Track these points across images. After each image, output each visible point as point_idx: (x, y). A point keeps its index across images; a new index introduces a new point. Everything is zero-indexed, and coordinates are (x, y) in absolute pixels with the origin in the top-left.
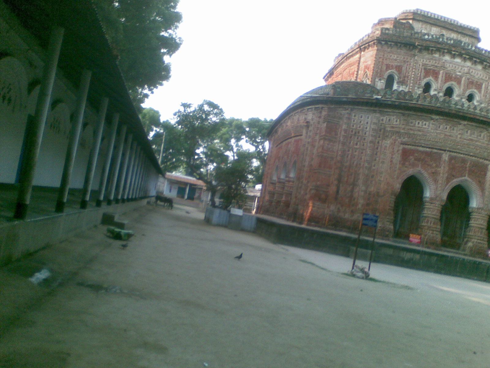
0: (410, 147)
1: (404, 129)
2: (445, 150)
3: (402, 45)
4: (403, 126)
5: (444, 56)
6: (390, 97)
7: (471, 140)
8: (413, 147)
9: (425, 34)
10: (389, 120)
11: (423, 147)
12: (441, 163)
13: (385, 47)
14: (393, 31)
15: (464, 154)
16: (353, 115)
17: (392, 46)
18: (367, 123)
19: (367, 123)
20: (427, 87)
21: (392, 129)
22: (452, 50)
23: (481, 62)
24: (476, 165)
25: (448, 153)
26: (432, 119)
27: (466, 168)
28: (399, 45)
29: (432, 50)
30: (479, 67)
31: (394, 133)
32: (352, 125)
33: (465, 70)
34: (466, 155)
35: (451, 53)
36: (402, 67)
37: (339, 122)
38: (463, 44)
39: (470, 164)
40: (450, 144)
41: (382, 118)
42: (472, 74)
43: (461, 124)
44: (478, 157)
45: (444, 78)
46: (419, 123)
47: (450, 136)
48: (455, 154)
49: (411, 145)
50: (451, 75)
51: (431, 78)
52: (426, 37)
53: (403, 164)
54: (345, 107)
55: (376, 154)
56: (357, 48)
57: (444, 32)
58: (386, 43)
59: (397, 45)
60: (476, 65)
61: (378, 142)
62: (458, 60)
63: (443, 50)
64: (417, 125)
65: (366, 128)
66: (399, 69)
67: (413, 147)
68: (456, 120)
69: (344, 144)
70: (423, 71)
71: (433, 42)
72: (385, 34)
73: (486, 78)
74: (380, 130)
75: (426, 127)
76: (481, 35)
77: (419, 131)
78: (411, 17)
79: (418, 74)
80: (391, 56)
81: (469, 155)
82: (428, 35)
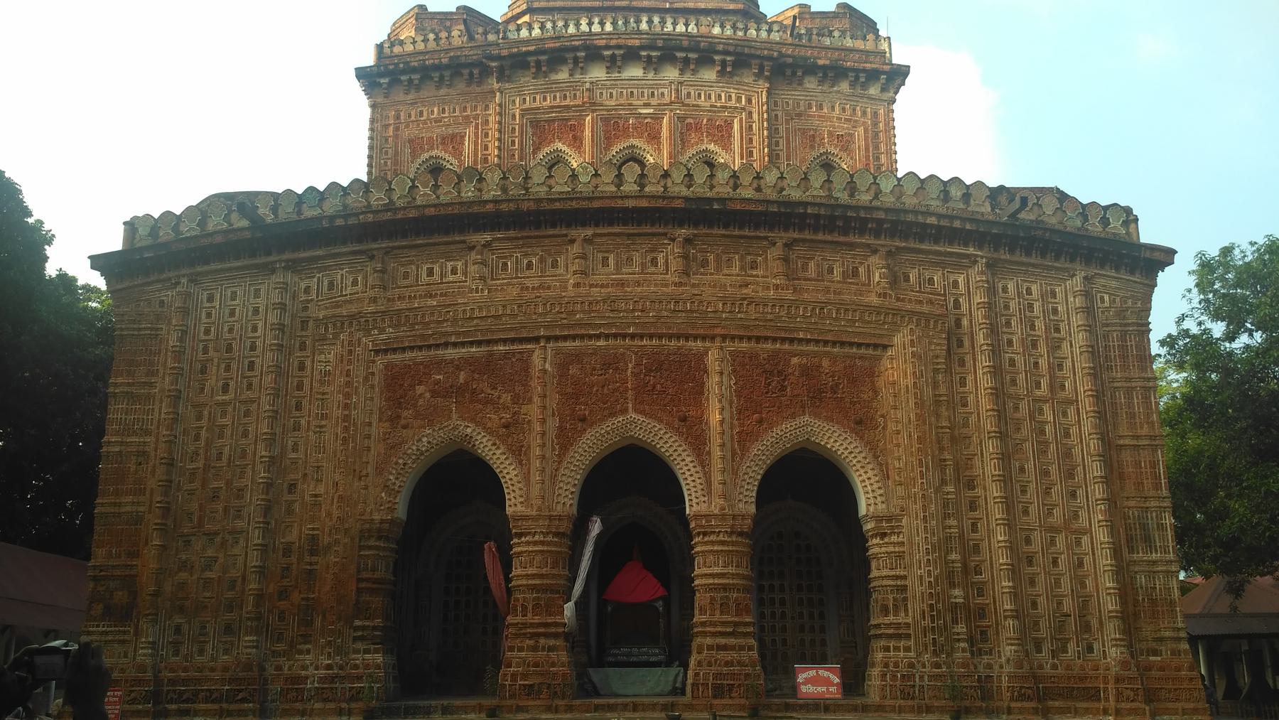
1: (374, 300)
2: (536, 340)
3: (447, 73)
4: (371, 293)
7: (622, 284)
8: (419, 355)
11: (455, 345)
12: (534, 383)
14: (414, 42)
15: (607, 337)
16: (205, 296)
17: (416, 82)
18: (256, 311)
19: (256, 311)
21: (330, 312)
26: (472, 248)
28: (436, 75)
30: (710, 75)
31: (343, 324)
33: (663, 94)
34: (615, 336)
35: (602, 58)
36: (463, 137)
37: (157, 329)
38: (644, 26)
40: (544, 314)
41: (303, 285)
42: (687, 101)
43: (572, 241)
44: (660, 337)
46: (430, 272)
47: (541, 287)
48: (577, 343)
49: (412, 348)
50: (621, 123)
51: (560, 146)
52: (524, 33)
53: (394, 420)
55: (299, 407)
58: (395, 82)
60: (694, 72)
61: (302, 367)
63: (571, 55)
65: (255, 329)
67: (419, 355)
68: (551, 232)
70: (529, 129)
73: (739, 99)
74: (304, 324)
75: (459, 276)
78: (524, 7)
79: (513, 142)
80: (421, 112)
81: (624, 336)
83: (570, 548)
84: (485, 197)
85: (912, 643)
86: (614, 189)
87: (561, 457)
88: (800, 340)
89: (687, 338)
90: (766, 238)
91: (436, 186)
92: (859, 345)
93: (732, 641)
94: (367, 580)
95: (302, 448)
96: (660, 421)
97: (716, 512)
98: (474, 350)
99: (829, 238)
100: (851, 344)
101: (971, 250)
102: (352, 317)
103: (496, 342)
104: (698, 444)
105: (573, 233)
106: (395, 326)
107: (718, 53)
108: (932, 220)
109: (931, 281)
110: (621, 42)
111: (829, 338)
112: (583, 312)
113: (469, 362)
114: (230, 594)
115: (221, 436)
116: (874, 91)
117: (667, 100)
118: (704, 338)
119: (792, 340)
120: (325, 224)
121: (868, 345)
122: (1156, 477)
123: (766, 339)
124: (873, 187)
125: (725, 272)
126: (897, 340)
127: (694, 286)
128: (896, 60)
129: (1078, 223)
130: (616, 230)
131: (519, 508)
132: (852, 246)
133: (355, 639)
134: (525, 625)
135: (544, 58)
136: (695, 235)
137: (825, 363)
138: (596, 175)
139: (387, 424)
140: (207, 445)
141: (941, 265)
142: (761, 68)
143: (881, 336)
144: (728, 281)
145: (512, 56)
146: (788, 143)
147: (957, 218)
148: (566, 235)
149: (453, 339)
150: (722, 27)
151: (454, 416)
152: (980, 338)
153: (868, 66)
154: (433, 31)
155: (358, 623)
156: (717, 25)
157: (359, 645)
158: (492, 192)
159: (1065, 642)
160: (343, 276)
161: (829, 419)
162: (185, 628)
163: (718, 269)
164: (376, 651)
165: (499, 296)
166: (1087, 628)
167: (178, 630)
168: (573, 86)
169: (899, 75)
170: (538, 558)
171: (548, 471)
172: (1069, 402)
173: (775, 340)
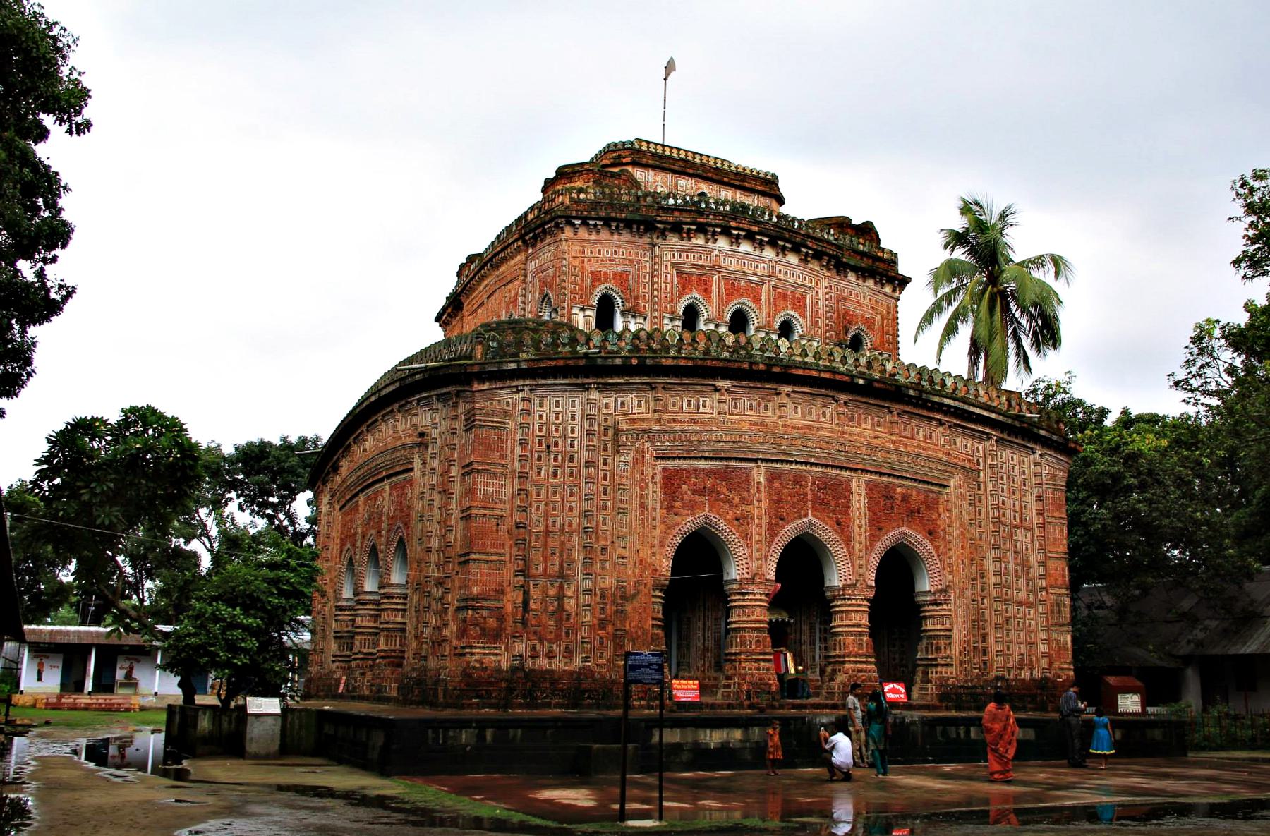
0: (677, 462)
2: (755, 460)
5: (715, 241)
6: (615, 348)
7: (810, 428)
9: (668, 196)
10: (623, 403)
11: (706, 458)
13: (583, 232)
15: (797, 462)
16: (537, 402)
18: (573, 418)
19: (573, 418)
20: (691, 315)
23: (796, 249)
24: (825, 485)
26: (717, 390)
27: (805, 494)
28: (614, 224)
29: (689, 230)
30: (793, 259)
32: (537, 427)
34: (802, 463)
39: (814, 483)
44: (827, 466)
45: (723, 290)
46: (689, 405)
48: (779, 465)
49: (680, 458)
51: (695, 294)
52: (671, 201)
53: (670, 508)
55: (605, 493)
56: (516, 240)
57: (705, 187)
58: (585, 223)
59: (610, 226)
60: (785, 255)
61: (605, 464)
62: (746, 247)
65: (573, 431)
66: (622, 278)
68: (768, 386)
69: (523, 477)
70: (676, 280)
71: (686, 211)
72: (579, 202)
76: (784, 188)
77: (694, 421)
78: (628, 160)
81: (806, 464)
82: (675, 198)
85: (953, 670)
89: (842, 468)
92: (932, 484)
93: (864, 666)
95: (608, 522)
100: (928, 483)
101: (990, 431)
102: (644, 431)
104: (848, 540)
105: (781, 388)
111: (918, 477)
115: (554, 509)
116: (888, 289)
117: (766, 272)
118: (851, 469)
119: (898, 477)
122: (1064, 576)
126: (952, 483)
128: (903, 269)
132: (932, 419)
134: (752, 653)
140: (547, 515)
141: (973, 437)
142: (829, 262)
144: (867, 433)
149: (706, 455)
152: (990, 487)
154: (607, 186)
159: (1021, 669)
160: (632, 399)
161: (916, 530)
162: (538, 647)
163: (860, 424)
166: (1031, 661)
167: (534, 648)
168: (708, 251)
169: (904, 282)
170: (758, 609)
172: (1029, 529)
173: (889, 475)
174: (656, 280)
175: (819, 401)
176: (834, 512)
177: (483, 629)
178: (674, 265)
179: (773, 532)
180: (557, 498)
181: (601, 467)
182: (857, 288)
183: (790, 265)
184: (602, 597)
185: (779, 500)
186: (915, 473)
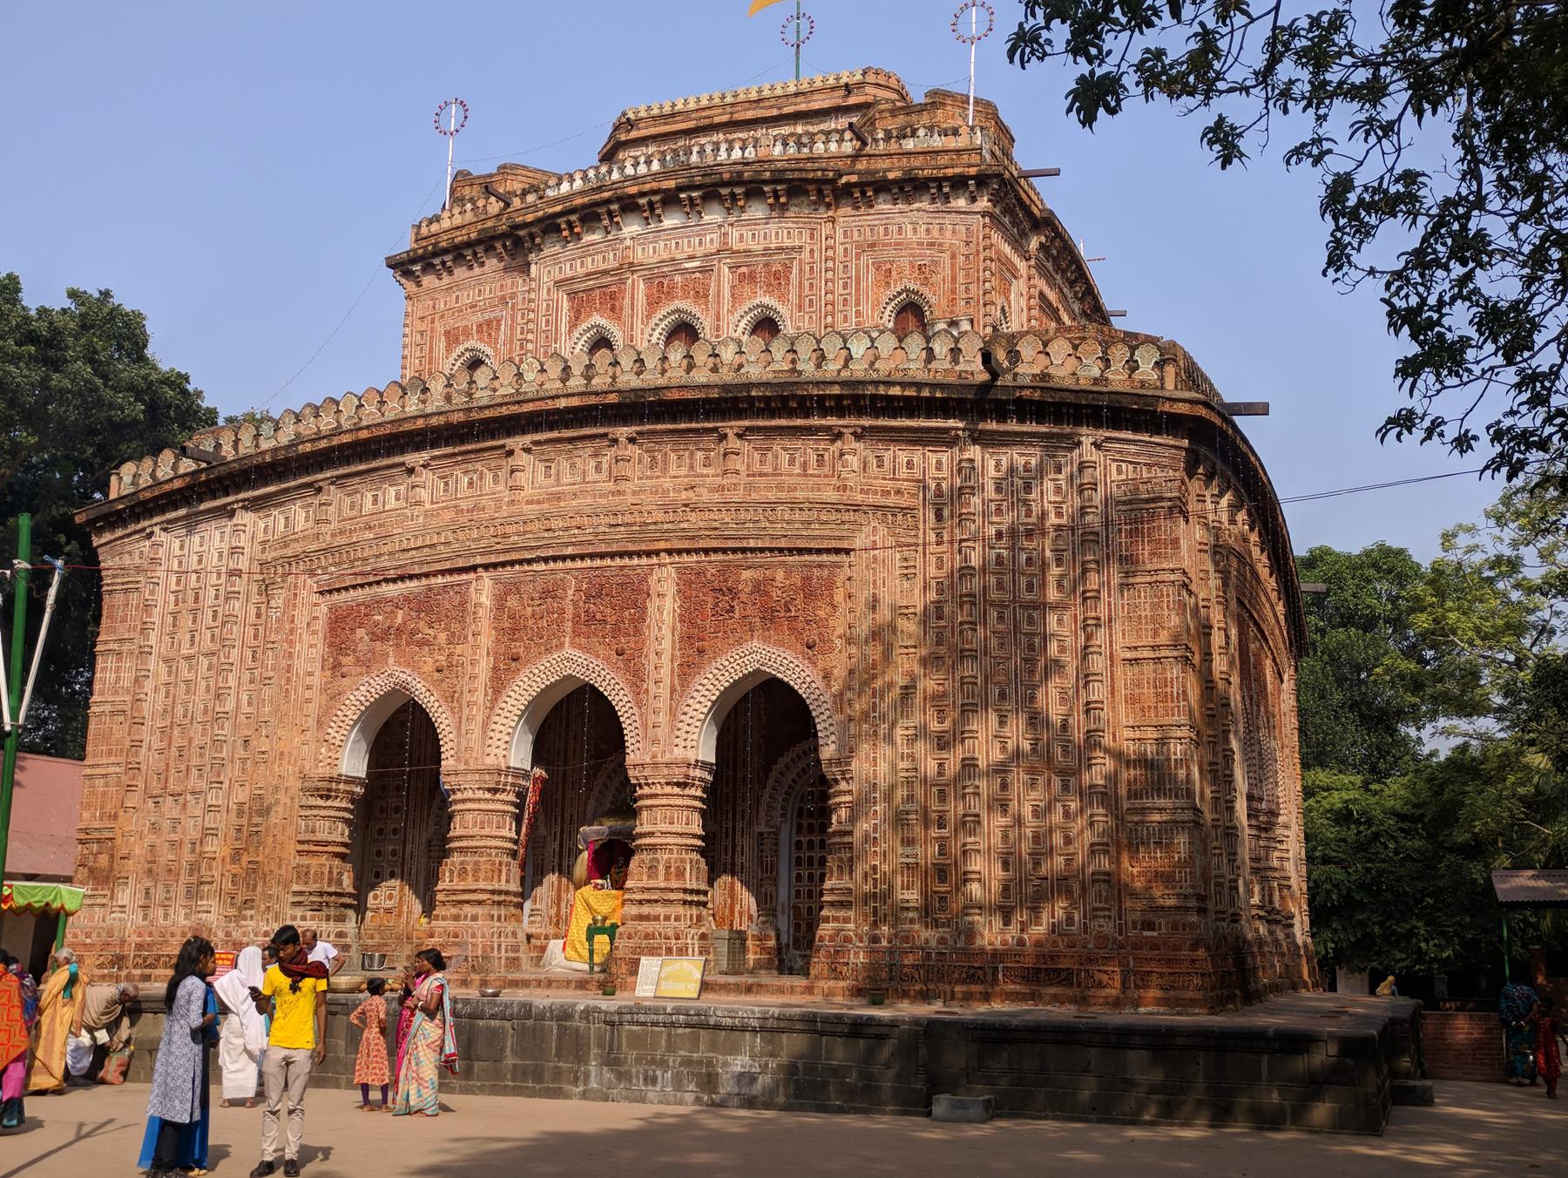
2: (474, 568)
3: (480, 249)
7: (558, 497)
11: (394, 581)
13: (429, 281)
15: (546, 560)
16: (177, 543)
19: (221, 554)
22: (633, 196)
25: (492, 573)
26: (411, 471)
27: (562, 612)
34: (555, 559)
36: (499, 321)
38: (694, 158)
43: (510, 453)
44: (602, 556)
49: (354, 587)
50: (666, 282)
51: (597, 319)
53: (336, 666)
54: (140, 526)
58: (428, 268)
63: (602, 210)
64: (368, 505)
66: (488, 328)
75: (402, 503)
81: (564, 558)
83: (516, 806)
84: (429, 410)
86: (559, 385)
87: (495, 700)
88: (752, 550)
89: (630, 554)
90: (715, 429)
91: (382, 403)
92: (819, 551)
94: (308, 842)
96: (598, 656)
97: (648, 760)
98: (414, 584)
99: (783, 422)
100: (809, 551)
103: (435, 574)
105: (510, 442)
106: (335, 564)
107: (766, 182)
108: (896, 391)
109: (910, 465)
110: (655, 185)
111: (783, 544)
112: (518, 534)
113: (407, 599)
114: (192, 858)
116: (961, 203)
118: (649, 554)
119: (743, 550)
120: (268, 458)
121: (828, 551)
123: (716, 550)
124: (844, 352)
125: (672, 473)
127: (634, 493)
129: (1096, 372)
130: (555, 434)
131: (451, 762)
133: (294, 904)
134: (454, 892)
135: (573, 218)
136: (639, 433)
137: (780, 575)
138: (543, 371)
139: (329, 673)
142: (820, 192)
143: (841, 538)
144: (667, 483)
145: (539, 220)
146: (858, 283)
147: (926, 384)
148: (503, 446)
150: (785, 144)
151: (391, 660)
153: (950, 172)
154: (472, 200)
155: (296, 888)
156: (779, 144)
157: (299, 912)
158: (436, 403)
162: (152, 891)
163: (665, 470)
164: (312, 919)
165: (434, 522)
171: (479, 719)
173: (724, 551)
174: (532, 316)
175: (587, 449)
176: (616, 629)
177: (91, 871)
178: (559, 284)
179: (498, 684)
180: (191, 676)
181: (252, 618)
182: (899, 219)
183: (753, 222)
184: (240, 813)
185: (514, 630)
186: (773, 537)
